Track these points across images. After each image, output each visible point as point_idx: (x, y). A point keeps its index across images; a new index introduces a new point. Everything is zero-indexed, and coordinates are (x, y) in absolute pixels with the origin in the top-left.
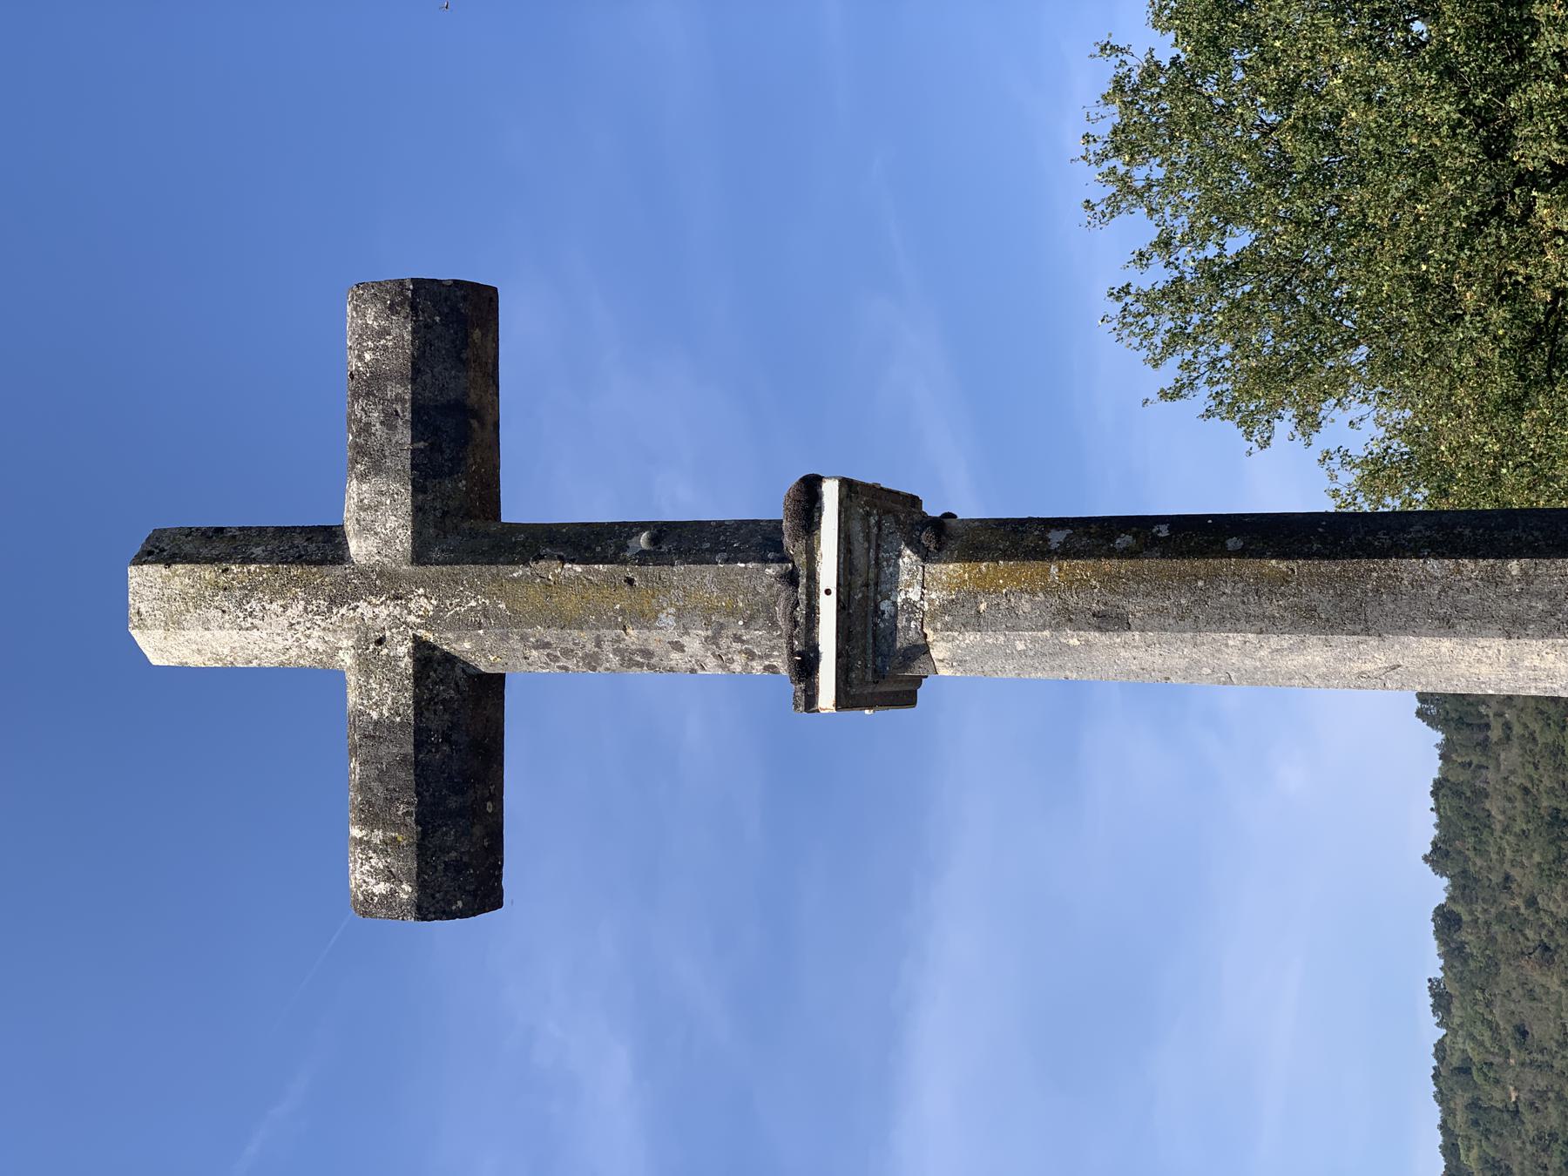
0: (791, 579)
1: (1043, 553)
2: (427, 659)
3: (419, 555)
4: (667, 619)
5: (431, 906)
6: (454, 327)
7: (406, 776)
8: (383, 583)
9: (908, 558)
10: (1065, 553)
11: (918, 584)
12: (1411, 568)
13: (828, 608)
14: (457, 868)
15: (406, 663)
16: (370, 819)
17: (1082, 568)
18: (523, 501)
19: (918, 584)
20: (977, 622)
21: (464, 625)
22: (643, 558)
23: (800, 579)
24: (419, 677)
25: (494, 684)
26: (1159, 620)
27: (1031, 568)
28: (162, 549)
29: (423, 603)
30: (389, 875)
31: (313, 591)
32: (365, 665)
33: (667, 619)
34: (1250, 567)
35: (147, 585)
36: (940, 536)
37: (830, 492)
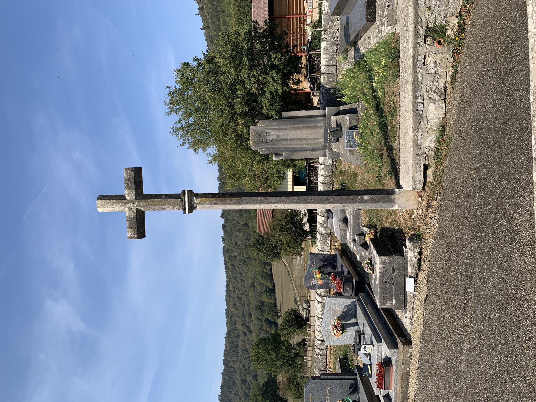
0: (182, 201)
1: (209, 197)
2: (137, 210)
3: (136, 199)
4: (167, 205)
5: (139, 238)
6: (138, 172)
7: (136, 223)
8: (131, 202)
9: (195, 198)
10: (211, 197)
11: (196, 201)
12: (244, 198)
13: (187, 204)
14: (141, 233)
15: (135, 211)
16: (131, 228)
17: (213, 199)
18: (146, 192)
19: (196, 201)
20: (202, 204)
21: (142, 206)
22: (164, 198)
23: (183, 201)
24: (137, 212)
25: (144, 212)
26: (221, 204)
27: (207, 199)
28: (100, 198)
29: (137, 204)
30: (134, 234)
31: (122, 203)
32: (129, 211)
33: (167, 205)
34: (229, 198)
35: (99, 202)
36: (197, 195)
37: (186, 192)
